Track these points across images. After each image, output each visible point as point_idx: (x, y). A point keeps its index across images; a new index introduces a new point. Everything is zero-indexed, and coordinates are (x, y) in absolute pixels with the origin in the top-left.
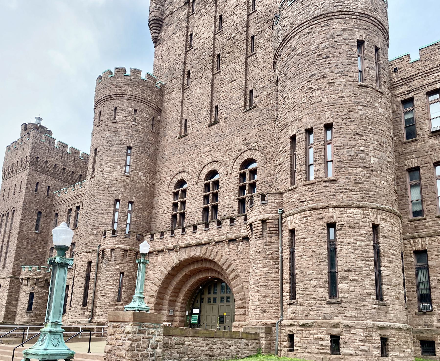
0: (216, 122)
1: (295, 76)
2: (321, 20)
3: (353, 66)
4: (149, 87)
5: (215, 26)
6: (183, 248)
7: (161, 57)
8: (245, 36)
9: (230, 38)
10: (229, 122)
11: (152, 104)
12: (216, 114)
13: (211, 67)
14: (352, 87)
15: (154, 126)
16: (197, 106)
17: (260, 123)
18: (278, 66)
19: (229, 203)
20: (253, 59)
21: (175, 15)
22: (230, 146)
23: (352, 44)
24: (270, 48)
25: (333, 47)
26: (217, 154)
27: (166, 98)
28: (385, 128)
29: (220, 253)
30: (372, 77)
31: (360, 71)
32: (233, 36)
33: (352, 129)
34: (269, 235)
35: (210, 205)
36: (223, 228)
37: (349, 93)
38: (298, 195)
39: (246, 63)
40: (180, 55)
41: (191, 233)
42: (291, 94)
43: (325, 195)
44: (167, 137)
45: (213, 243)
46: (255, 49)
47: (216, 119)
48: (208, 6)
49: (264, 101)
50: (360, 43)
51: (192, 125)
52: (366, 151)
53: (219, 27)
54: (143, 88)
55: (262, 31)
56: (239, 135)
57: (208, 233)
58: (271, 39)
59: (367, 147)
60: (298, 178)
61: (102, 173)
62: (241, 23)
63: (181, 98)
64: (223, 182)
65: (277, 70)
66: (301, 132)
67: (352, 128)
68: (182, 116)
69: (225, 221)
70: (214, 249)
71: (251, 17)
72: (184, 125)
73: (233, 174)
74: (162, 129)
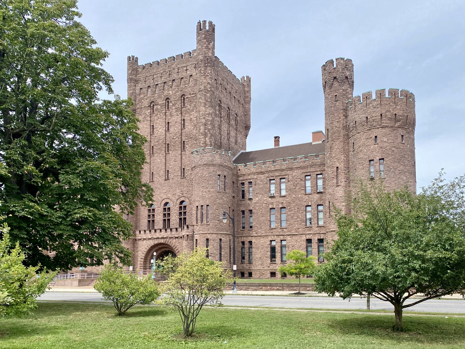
0: (168, 179)
12: (168, 174)
26: (169, 195)
35: (166, 218)
47: (168, 176)
67: (215, 207)
68: (150, 170)
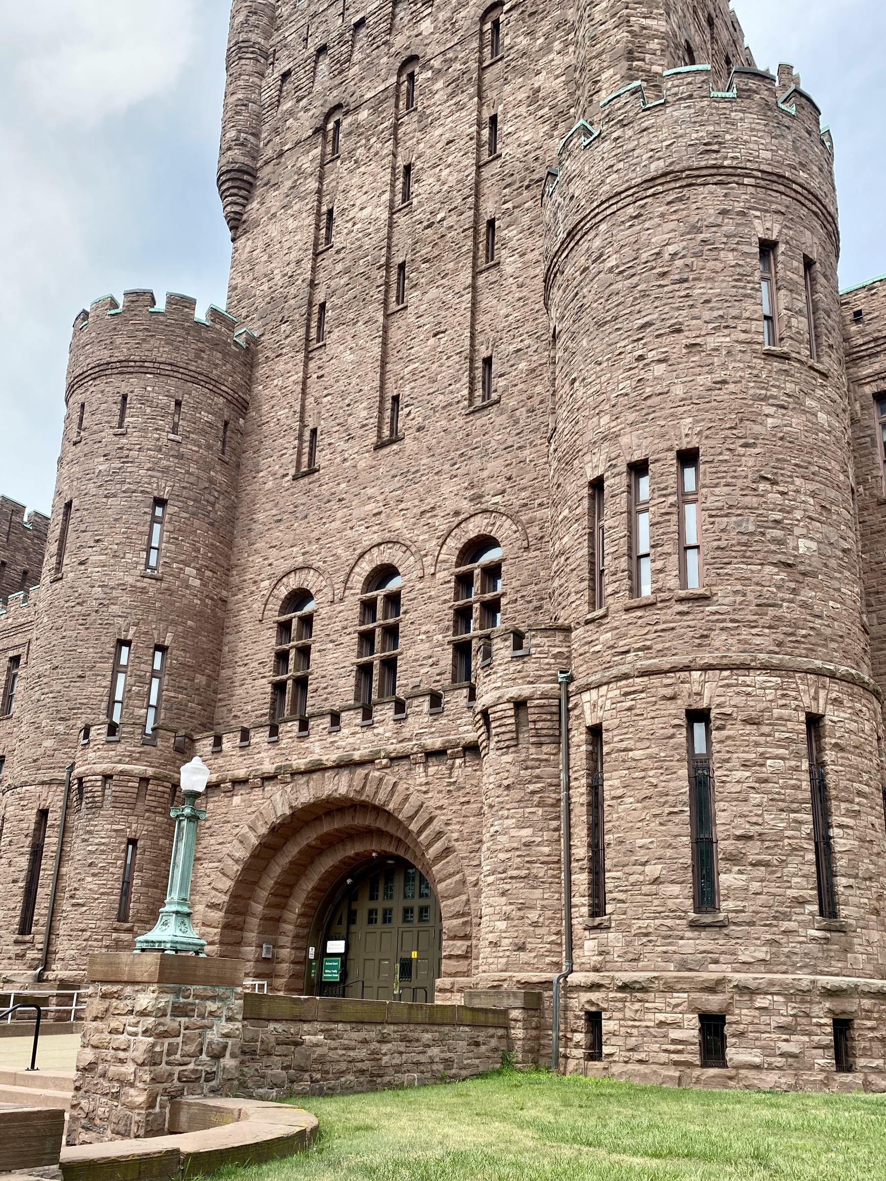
0: (395, 438)
1: (600, 325)
2: (666, 187)
3: (748, 304)
4: (215, 344)
5: (393, 192)
6: (303, 773)
7: (248, 267)
8: (472, 219)
9: (433, 223)
10: (428, 438)
11: (223, 388)
13: (381, 297)
14: (747, 357)
15: (227, 444)
16: (343, 395)
17: (510, 444)
18: (557, 300)
19: (429, 653)
20: (492, 278)
21: (288, 161)
22: (431, 501)
23: (746, 249)
24: (536, 252)
25: (696, 255)
26: (398, 523)
27: (262, 371)
28: (833, 463)
29: (401, 787)
30: (798, 333)
31: (766, 318)
32: (439, 217)
33: (750, 464)
34: (533, 740)
35: (376, 658)
36: (410, 719)
37: (740, 373)
38: (609, 635)
39: (474, 287)
40: (298, 262)
41: (325, 732)
42: (590, 371)
43: (681, 637)
44: (261, 474)
45: (384, 761)
46: (496, 252)
47: (393, 429)
48: (374, 139)
49: (520, 386)
50: (767, 248)
51: (330, 444)
52: (786, 521)
53: (404, 194)
54: (200, 345)
55: (514, 208)
56: (454, 473)
57: (369, 734)
58: (540, 229)
59: (788, 512)
60: (609, 590)
61: (83, 567)
62: (459, 187)
63: (301, 374)
64: (412, 595)
65: (553, 309)
66: (616, 471)
67: (749, 461)
68: (302, 419)
69: (416, 702)
70: (387, 777)
71: (486, 173)
72: (307, 444)
73: (437, 575)
74: (249, 453)
